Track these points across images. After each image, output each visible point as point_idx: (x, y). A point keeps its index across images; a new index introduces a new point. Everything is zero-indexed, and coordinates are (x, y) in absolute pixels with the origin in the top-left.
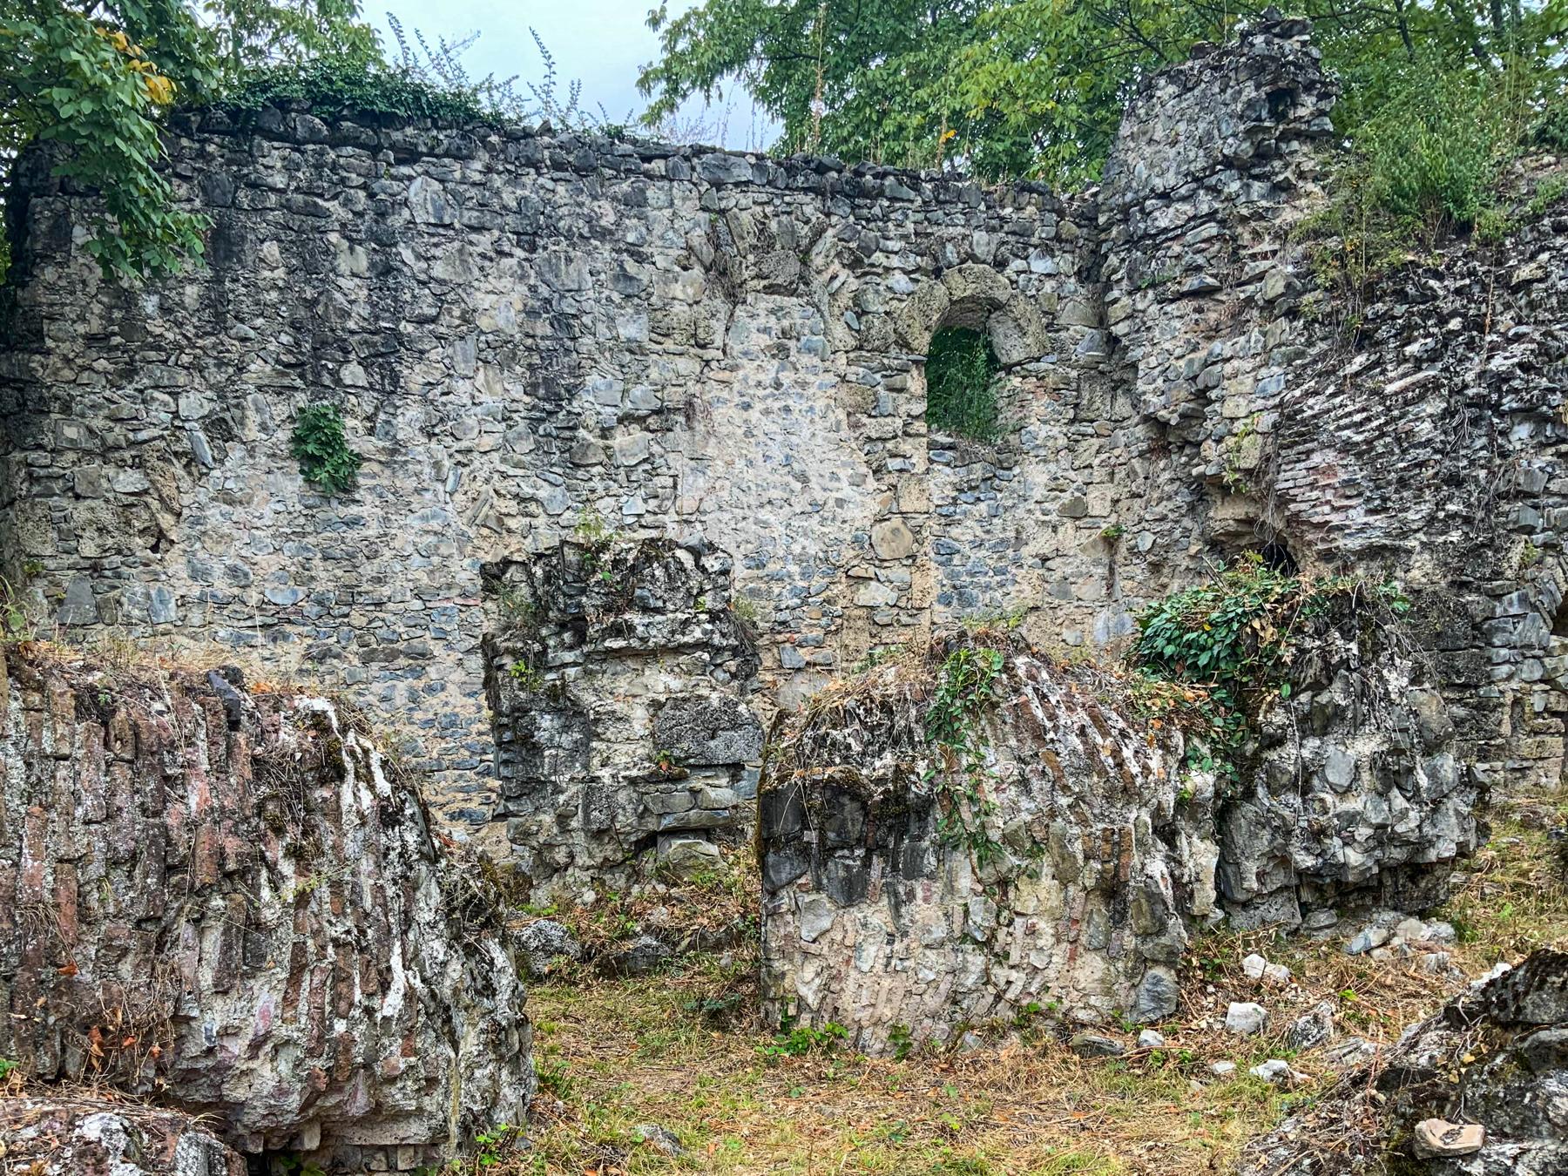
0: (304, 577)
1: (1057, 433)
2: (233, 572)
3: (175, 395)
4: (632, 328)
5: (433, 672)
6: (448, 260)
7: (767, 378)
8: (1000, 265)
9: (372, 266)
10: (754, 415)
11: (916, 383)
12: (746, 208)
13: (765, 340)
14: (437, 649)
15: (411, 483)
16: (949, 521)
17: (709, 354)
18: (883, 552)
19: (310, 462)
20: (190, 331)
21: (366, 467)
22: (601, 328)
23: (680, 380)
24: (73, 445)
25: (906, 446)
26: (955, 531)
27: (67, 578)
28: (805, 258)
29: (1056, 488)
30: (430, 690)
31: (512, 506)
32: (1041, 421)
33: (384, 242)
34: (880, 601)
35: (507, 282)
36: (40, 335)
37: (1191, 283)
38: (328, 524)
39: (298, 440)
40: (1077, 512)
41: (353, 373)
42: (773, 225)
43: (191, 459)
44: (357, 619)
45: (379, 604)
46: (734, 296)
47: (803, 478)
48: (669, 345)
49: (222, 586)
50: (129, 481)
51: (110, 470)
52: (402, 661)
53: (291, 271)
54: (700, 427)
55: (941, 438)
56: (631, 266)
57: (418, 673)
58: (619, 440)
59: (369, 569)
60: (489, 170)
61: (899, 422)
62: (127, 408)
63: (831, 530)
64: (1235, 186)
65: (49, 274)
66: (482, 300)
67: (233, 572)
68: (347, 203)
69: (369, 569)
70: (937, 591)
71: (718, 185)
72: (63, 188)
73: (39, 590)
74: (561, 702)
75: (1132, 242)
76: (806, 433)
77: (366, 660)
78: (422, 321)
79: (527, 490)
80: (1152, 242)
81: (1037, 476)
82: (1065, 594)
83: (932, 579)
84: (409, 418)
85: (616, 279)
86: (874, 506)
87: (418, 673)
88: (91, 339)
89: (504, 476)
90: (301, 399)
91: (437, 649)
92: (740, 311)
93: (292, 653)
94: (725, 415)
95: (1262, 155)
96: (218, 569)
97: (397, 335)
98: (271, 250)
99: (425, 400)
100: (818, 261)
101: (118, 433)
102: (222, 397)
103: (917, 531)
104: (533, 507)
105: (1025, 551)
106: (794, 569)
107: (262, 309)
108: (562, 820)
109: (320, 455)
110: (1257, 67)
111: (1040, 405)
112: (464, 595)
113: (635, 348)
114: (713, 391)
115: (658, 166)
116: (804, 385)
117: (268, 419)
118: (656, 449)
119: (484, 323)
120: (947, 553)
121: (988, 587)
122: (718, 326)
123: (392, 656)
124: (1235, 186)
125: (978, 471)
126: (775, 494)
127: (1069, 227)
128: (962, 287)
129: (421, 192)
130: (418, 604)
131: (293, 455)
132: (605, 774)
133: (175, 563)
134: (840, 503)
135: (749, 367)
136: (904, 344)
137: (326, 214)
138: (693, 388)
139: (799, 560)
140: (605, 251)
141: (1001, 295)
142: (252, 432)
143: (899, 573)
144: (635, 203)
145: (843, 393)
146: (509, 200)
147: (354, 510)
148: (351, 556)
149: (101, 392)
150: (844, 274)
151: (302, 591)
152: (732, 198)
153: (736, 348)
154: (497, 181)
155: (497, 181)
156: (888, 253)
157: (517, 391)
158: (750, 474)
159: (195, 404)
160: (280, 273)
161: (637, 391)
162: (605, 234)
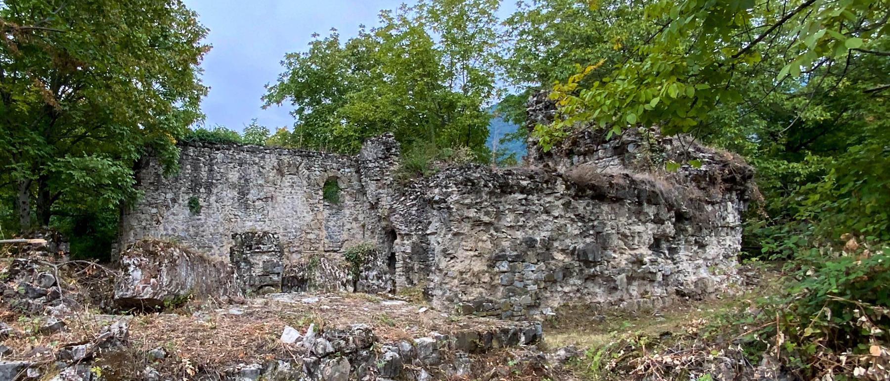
0: (187, 230)
2: (173, 229)
14: (214, 246)
19: (192, 208)
27: (138, 230)
39: (189, 203)
43: (167, 207)
44: (198, 239)
49: (170, 232)
50: (154, 211)
58: (257, 203)
59: (201, 229)
62: (156, 196)
67: (173, 229)
69: (201, 229)
73: (132, 233)
84: (213, 198)
88: (150, 183)
90: (191, 195)
91: (214, 246)
101: (153, 201)
109: (194, 206)
117: (184, 199)
133: (161, 227)
142: (180, 201)
159: (170, 196)
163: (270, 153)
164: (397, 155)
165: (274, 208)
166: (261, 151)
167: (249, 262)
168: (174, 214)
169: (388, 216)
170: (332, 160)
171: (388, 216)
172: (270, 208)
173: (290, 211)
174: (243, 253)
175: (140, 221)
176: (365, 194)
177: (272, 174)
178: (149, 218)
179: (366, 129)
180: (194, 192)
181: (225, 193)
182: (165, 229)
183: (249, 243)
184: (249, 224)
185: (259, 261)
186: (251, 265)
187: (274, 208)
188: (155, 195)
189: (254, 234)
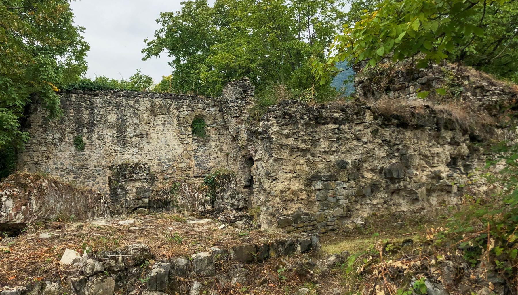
0: (74, 164)
1: (216, 137)
3: (53, 135)
4: (135, 121)
5: (97, 180)
6: (103, 111)
7: (161, 129)
8: (205, 109)
9: (89, 113)
10: (159, 135)
11: (189, 129)
12: (158, 102)
13: (161, 122)
15: (95, 148)
16: (197, 152)
17: (150, 125)
18: (184, 158)
19: (76, 145)
20: (57, 124)
21: (86, 145)
22: (131, 121)
23: (145, 129)
24: (35, 143)
25: (188, 139)
26: (198, 154)
28: (168, 109)
29: (217, 146)
30: (96, 183)
31: (113, 151)
32: (213, 135)
33: (92, 109)
34: (183, 166)
35: (114, 114)
36: (30, 125)
37: (235, 115)
38: (79, 155)
39: (74, 141)
40: (221, 150)
41: (85, 130)
42: (162, 104)
44: (83, 171)
45: (87, 169)
46: (155, 115)
47: (168, 145)
48: (143, 123)
49: (59, 166)
50: (44, 149)
51: (41, 147)
52: (91, 178)
53: (75, 114)
54: (149, 137)
55: (195, 138)
56: (136, 111)
57: (94, 180)
58: (133, 139)
59: (86, 163)
60: (111, 97)
61: (186, 136)
62: (44, 136)
63: (174, 154)
64: (240, 102)
65: (33, 116)
66: (109, 117)
67: (61, 164)
68: (86, 103)
69: (86, 163)
70: (194, 164)
71: (152, 98)
72: (37, 102)
75: (227, 107)
76: (169, 138)
77: (84, 178)
78: (98, 121)
79: (116, 148)
80: (230, 108)
81: (213, 144)
82: (219, 164)
83: (193, 162)
85: (133, 113)
86: (182, 150)
87: (94, 180)
88: (39, 126)
89: (112, 146)
90: (76, 135)
92: (156, 118)
93: (71, 177)
94: (153, 135)
95: (244, 98)
96: (59, 163)
97: (93, 124)
98: (72, 111)
99: (98, 134)
100: (171, 109)
101: (43, 141)
102: (61, 134)
103: (190, 154)
104: (117, 151)
105: (211, 157)
106: (167, 161)
107: (70, 120)
108: (121, 206)
109: (79, 144)
110: (241, 86)
111: (213, 132)
112: (103, 167)
113: (137, 124)
114: (151, 131)
115: (141, 95)
116: (168, 130)
117: (70, 138)
118: (140, 141)
119: (109, 121)
120: (196, 158)
121: (204, 163)
122: (152, 120)
123: (89, 178)
124: (240, 102)
125: (202, 143)
126: (163, 148)
127: (217, 103)
128: (198, 113)
129: (99, 101)
130: (95, 168)
131: (73, 144)
132: (129, 198)
133: (51, 162)
134: (175, 149)
135: (158, 127)
136: (187, 122)
137: (82, 105)
138: (147, 130)
139: (167, 159)
140: (132, 109)
141: (205, 114)
142: (67, 140)
143: (187, 161)
144: (137, 101)
145: (176, 131)
146: (114, 101)
147: (84, 152)
148: (83, 160)
149: (40, 134)
150: (176, 111)
151: (73, 167)
152: (155, 100)
153: (156, 124)
154: (112, 99)
155: (112, 99)
156: (184, 108)
157: (115, 132)
158: (158, 145)
159: (57, 136)
160: (73, 114)
161: (137, 131)
162: (131, 106)
163: (144, 97)
164: (252, 96)
165: (149, 143)
166: (135, 96)
167: (124, 189)
168: (61, 151)
169: (247, 146)
170: (198, 101)
171: (247, 146)
172: (145, 143)
173: (163, 146)
174: (119, 181)
175: (32, 158)
176: (227, 129)
177: (146, 115)
178: (39, 155)
179: (229, 74)
180: (78, 132)
181: (105, 132)
182: (55, 164)
183: (123, 173)
184: (130, 157)
185: (133, 188)
186: (126, 191)
187: (149, 143)
188: (44, 135)
189: (127, 165)
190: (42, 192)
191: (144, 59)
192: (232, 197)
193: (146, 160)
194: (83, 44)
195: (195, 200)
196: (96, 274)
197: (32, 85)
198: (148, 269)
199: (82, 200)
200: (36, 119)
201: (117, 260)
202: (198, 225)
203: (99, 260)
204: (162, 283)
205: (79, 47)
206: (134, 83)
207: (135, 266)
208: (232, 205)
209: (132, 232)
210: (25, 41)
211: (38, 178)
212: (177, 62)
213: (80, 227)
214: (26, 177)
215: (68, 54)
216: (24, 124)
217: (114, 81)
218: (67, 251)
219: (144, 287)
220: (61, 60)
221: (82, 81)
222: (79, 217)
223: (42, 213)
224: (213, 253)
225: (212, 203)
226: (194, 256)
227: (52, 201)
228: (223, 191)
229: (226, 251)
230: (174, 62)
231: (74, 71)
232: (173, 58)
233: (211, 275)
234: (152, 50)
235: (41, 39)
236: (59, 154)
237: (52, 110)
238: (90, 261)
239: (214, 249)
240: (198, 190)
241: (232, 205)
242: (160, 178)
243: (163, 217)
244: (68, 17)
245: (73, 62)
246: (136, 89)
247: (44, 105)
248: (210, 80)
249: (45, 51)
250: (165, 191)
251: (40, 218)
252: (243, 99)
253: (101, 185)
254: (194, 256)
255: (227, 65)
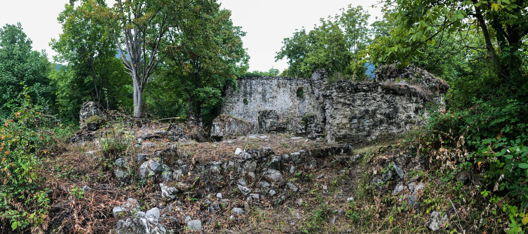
74: (264, 121)
94: (279, 97)
110: (321, 73)
144: (271, 81)
184: (268, 107)
190: (230, 123)
191: (276, 61)
192: (315, 127)
193: (275, 109)
194: (247, 56)
195: (297, 128)
196: (249, 159)
197: (226, 77)
198: (271, 159)
199: (246, 127)
200: (228, 92)
201: (257, 154)
202: (296, 140)
203: (250, 154)
204: (277, 166)
205: (246, 58)
206: (270, 73)
207: (265, 157)
208: (315, 130)
209: (264, 141)
210: (223, 58)
211: (228, 117)
212: (291, 61)
213: (244, 139)
214: (224, 117)
215: (241, 62)
216: (223, 94)
217: (261, 72)
218: (238, 148)
219: (269, 167)
220: (238, 64)
221: (247, 74)
222: (245, 134)
223: (230, 132)
224: (301, 153)
225: (306, 129)
226: (292, 154)
227: (234, 127)
228: (311, 123)
229: (307, 152)
230: (290, 62)
231: (243, 69)
232: (289, 60)
233: (300, 163)
234: (280, 57)
235: (229, 56)
236: (237, 107)
237: (234, 87)
238: (246, 154)
239: (302, 151)
240: (299, 123)
241: (315, 130)
242: (282, 117)
243: (280, 135)
244: (240, 45)
245: (243, 65)
246: (271, 76)
247: (231, 86)
248: (306, 70)
249: (231, 61)
250: (283, 123)
251: (229, 134)
252: (322, 79)
253: (255, 120)
254: (292, 154)
255: (314, 63)
